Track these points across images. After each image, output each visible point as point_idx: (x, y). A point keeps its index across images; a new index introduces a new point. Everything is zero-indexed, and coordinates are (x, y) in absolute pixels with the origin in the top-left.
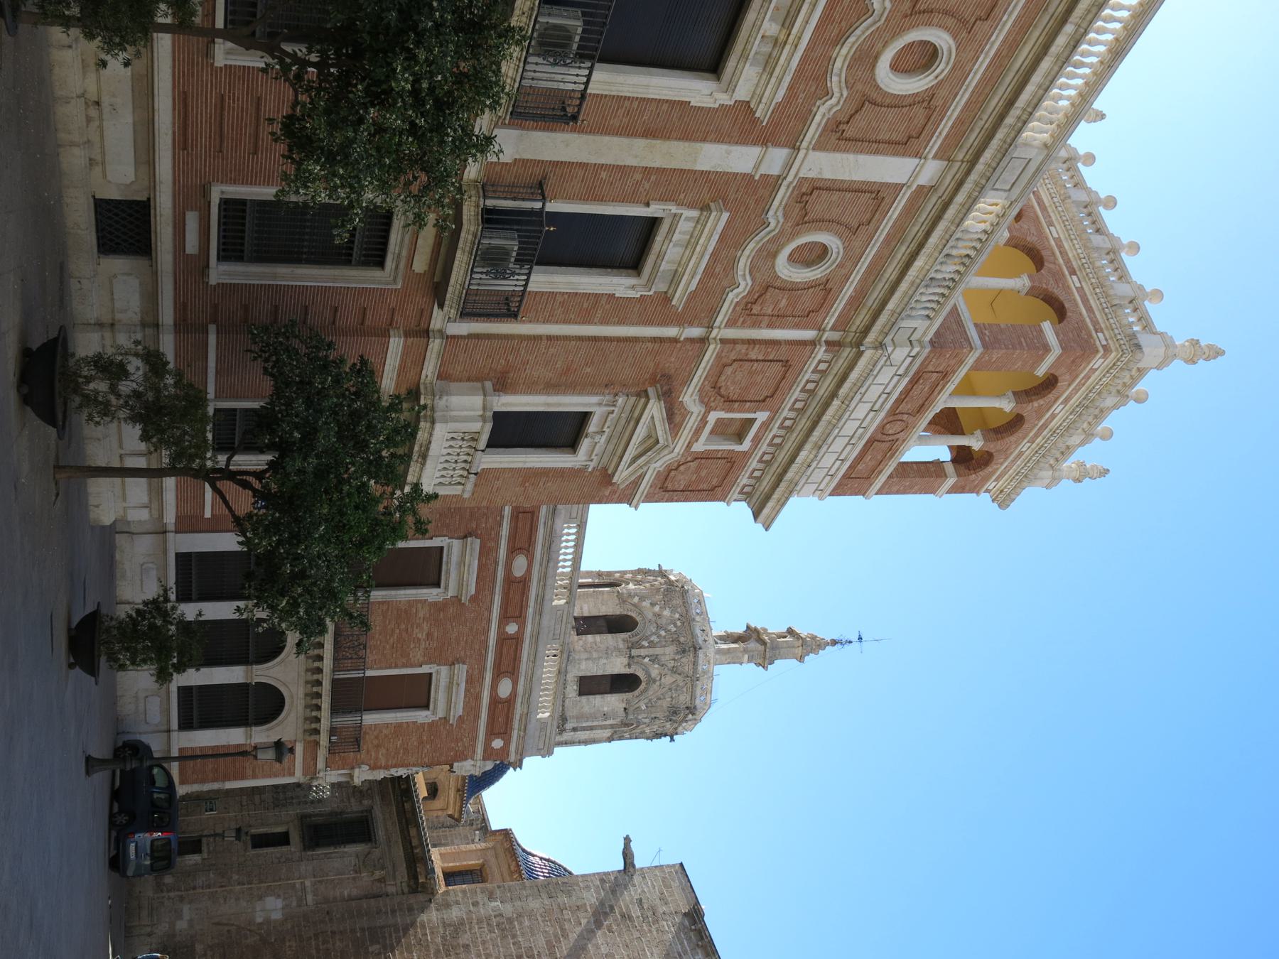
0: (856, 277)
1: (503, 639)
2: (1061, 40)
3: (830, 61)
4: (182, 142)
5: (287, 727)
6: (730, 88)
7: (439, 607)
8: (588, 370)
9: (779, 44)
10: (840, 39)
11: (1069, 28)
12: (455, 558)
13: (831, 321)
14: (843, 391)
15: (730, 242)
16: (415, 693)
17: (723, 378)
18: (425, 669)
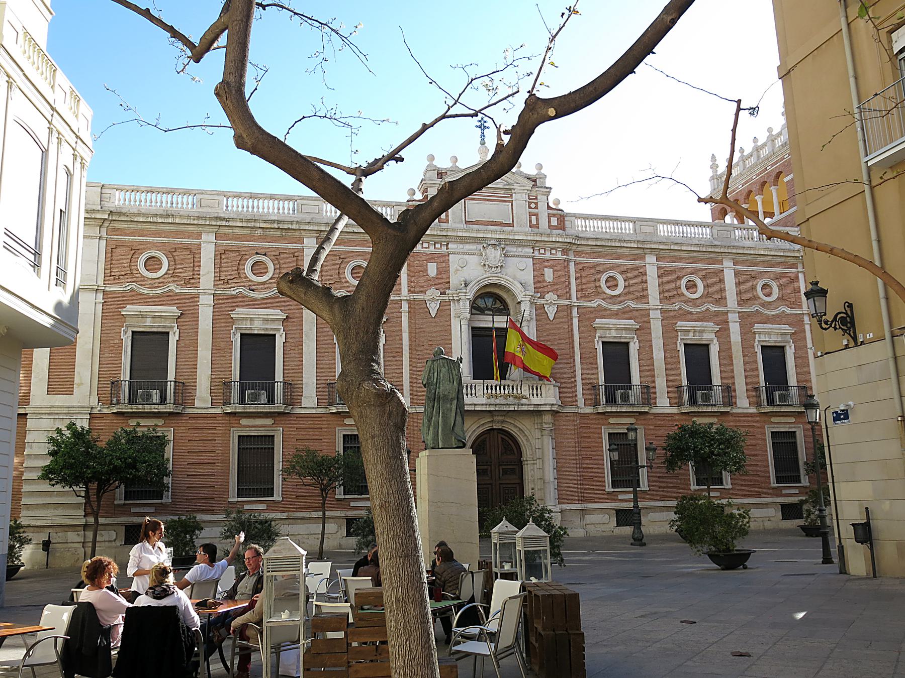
0: (773, 270)
2: (676, 248)
3: (697, 313)
4: (759, 495)
6: (712, 340)
9: (695, 331)
10: (690, 313)
13: (794, 270)
15: (766, 320)
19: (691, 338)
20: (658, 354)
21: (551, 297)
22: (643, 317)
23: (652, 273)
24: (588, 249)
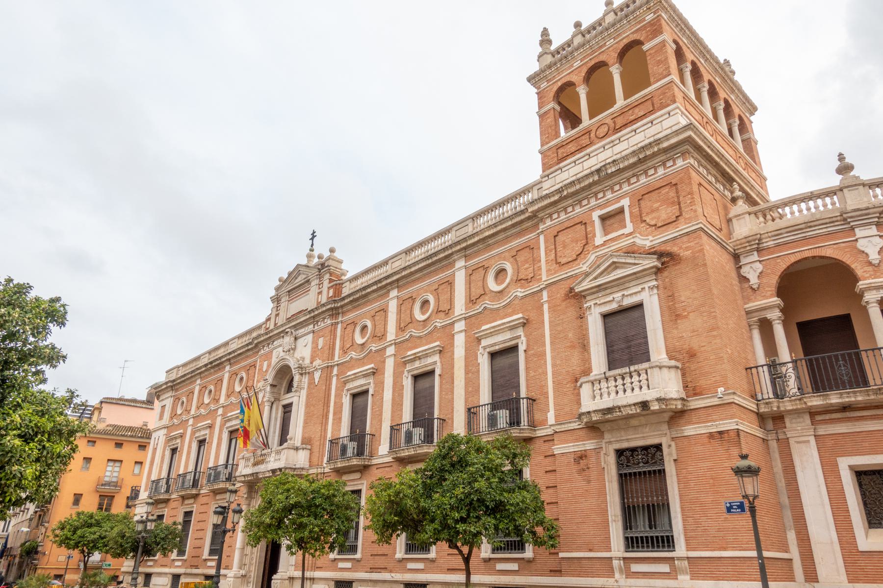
8: (570, 335)
11: (404, 273)
14: (556, 198)
15: (495, 313)
17: (570, 259)
20: (388, 395)
21: (317, 362)
23: (393, 306)
24: (350, 307)
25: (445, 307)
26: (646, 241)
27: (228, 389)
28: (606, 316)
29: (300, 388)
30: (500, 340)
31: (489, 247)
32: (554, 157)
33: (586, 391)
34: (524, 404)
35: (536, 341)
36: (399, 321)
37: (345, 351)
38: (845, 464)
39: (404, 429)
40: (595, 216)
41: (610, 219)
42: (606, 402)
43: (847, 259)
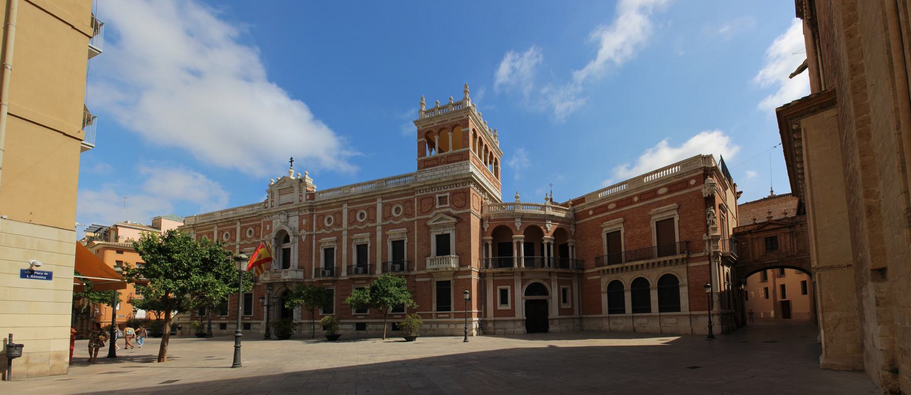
1: (640, 200)
5: (680, 272)
7: (627, 228)
12: (609, 229)
16: (665, 226)
18: (653, 225)
19: (359, 242)
20: (344, 252)
21: (303, 231)
22: (339, 235)
23: (345, 212)
25: (372, 218)
26: (454, 212)
27: (241, 235)
28: (437, 236)
29: (294, 242)
30: (397, 238)
31: (393, 197)
32: (424, 164)
33: (428, 262)
34: (405, 263)
35: (411, 240)
36: (349, 220)
37: (319, 228)
38: (499, 288)
39: (354, 267)
40: (437, 196)
41: (442, 200)
42: (435, 266)
43: (511, 227)
